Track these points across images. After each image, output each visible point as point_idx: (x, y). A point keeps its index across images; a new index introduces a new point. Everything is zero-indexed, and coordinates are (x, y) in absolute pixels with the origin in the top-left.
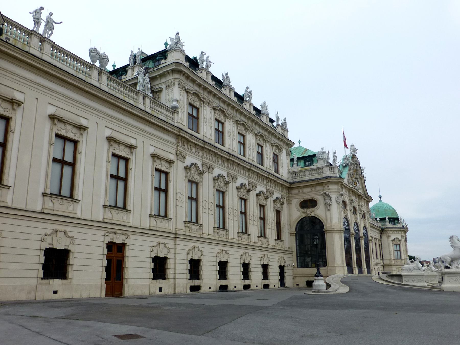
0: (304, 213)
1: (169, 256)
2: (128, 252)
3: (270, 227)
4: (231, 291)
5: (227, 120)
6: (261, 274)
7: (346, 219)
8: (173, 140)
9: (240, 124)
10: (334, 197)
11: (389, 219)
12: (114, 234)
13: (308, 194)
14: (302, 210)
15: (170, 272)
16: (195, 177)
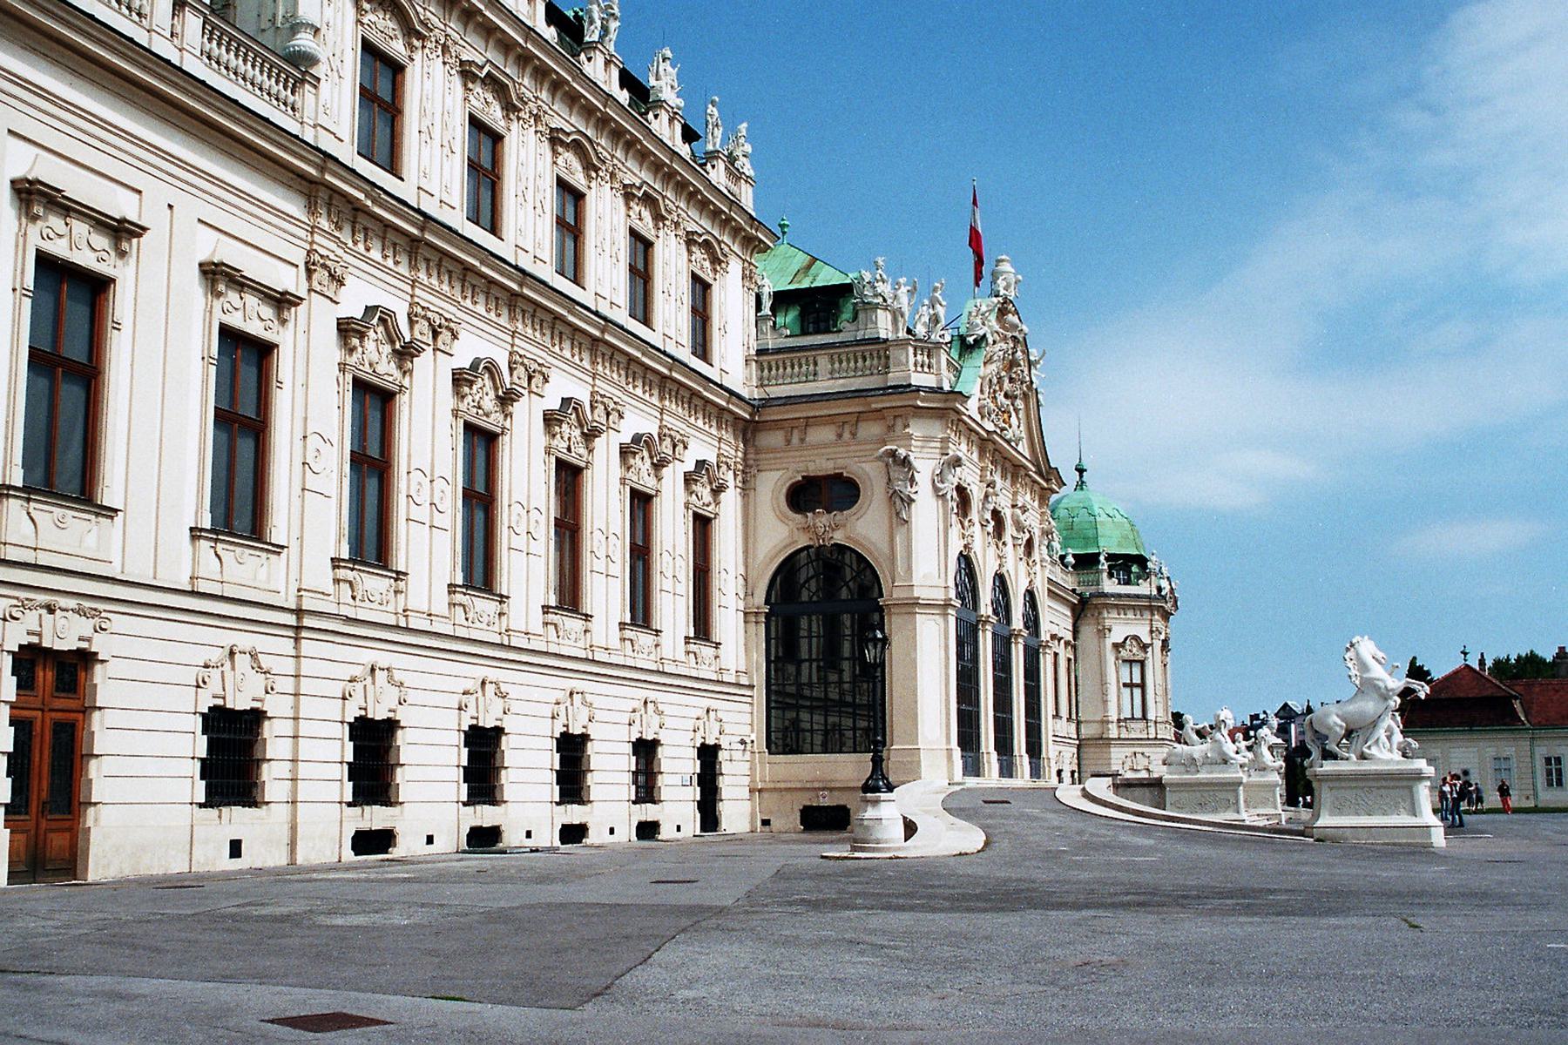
0: (806, 529)
1: (271, 706)
2: (106, 685)
3: (668, 584)
4: (518, 850)
5: (515, 126)
6: (628, 778)
7: (966, 561)
8: (293, 206)
9: (567, 146)
10: (925, 466)
12: (44, 612)
13: (822, 453)
14: (799, 517)
15: (273, 778)
16: (380, 369)
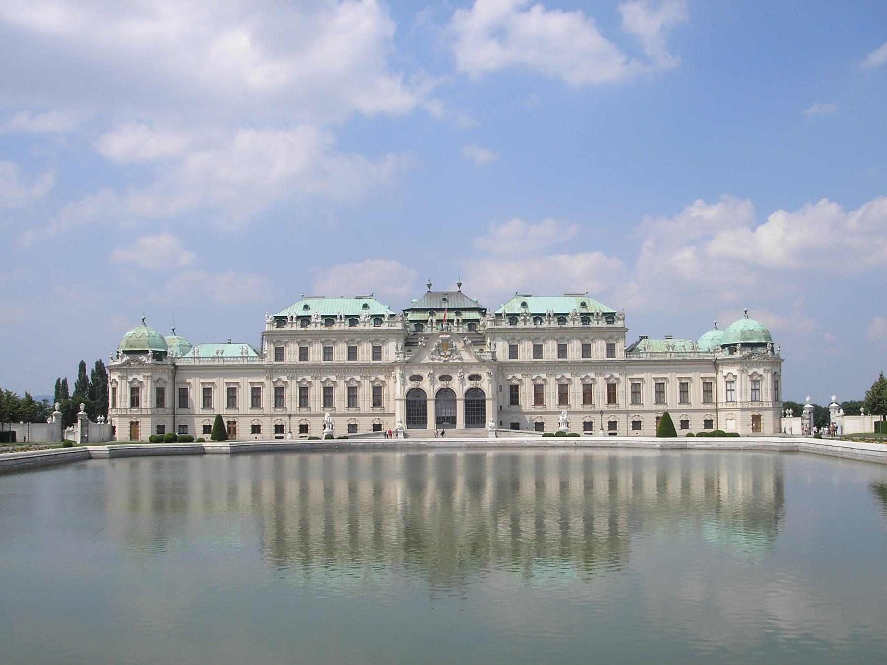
11: (723, 347)
